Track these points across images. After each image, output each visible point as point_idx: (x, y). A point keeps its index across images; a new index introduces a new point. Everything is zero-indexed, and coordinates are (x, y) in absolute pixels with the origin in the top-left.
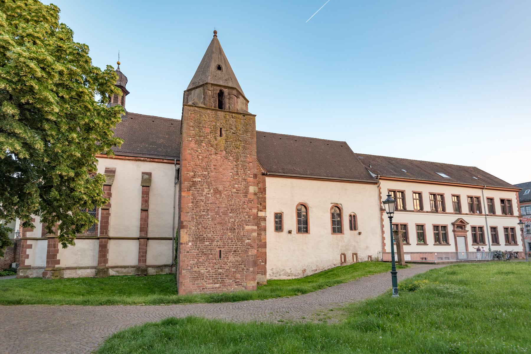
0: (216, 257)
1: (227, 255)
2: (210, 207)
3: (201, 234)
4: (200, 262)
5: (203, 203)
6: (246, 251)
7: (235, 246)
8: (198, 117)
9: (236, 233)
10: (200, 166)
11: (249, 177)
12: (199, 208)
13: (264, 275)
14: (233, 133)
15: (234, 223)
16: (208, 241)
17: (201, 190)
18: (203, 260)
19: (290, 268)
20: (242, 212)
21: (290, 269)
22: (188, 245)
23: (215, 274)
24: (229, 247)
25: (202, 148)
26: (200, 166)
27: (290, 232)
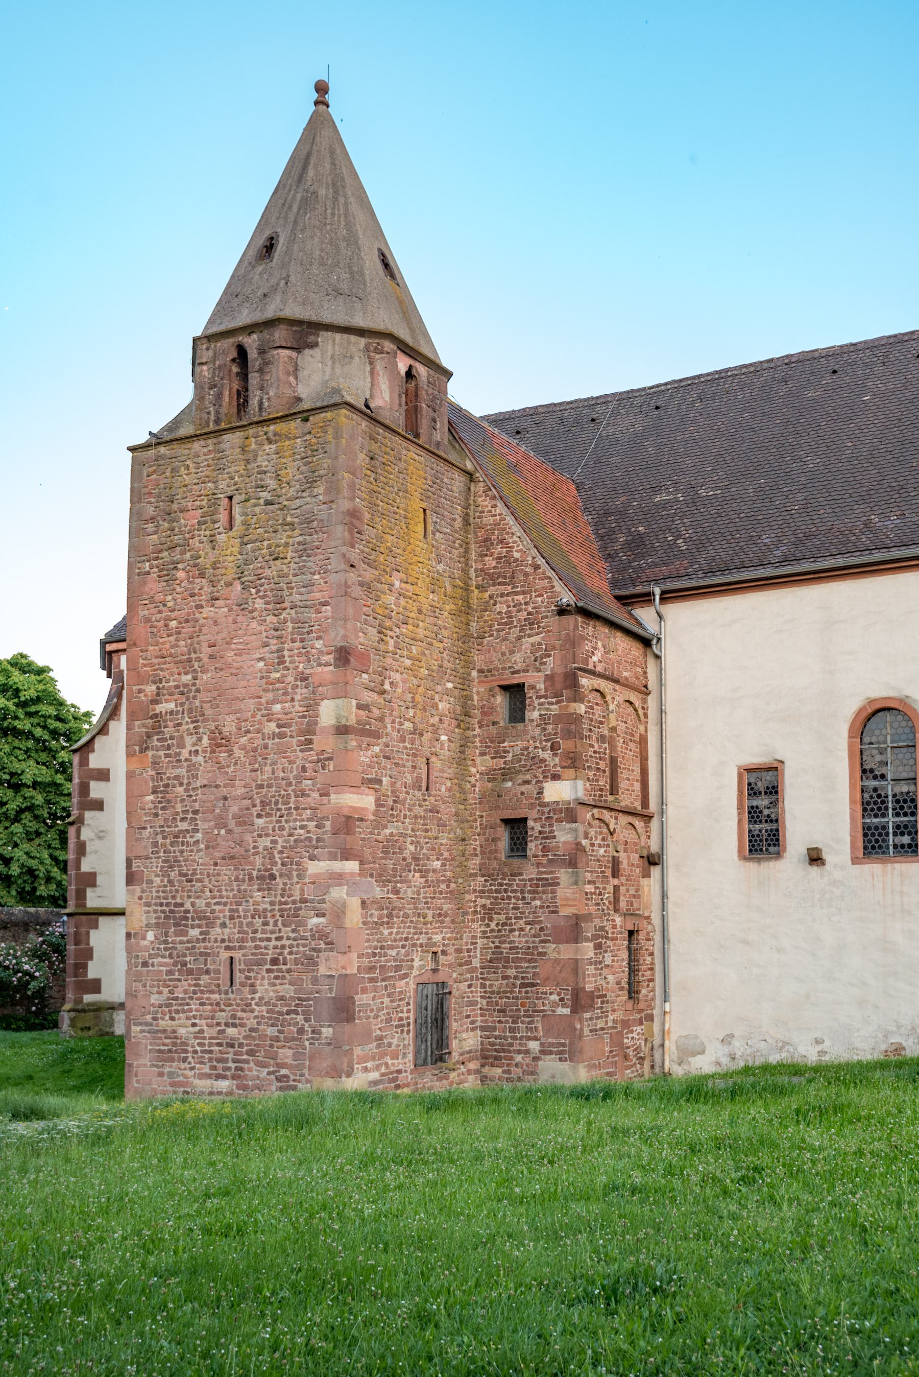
0: (220, 982)
1: (252, 974)
2: (200, 799)
3: (178, 900)
4: (176, 999)
5: (180, 790)
6: (312, 962)
7: (274, 943)
8: (166, 481)
9: (279, 892)
10: (171, 655)
11: (320, 665)
12: (172, 810)
13: (571, 1060)
14: (268, 503)
15: (269, 852)
16: (199, 926)
17: (174, 742)
18: (185, 992)
19: (818, 1035)
20: (297, 809)
21: (818, 1042)
22: (144, 938)
23: (219, 1044)
24: (256, 947)
25: (179, 589)
26: (171, 655)
27: (815, 858)
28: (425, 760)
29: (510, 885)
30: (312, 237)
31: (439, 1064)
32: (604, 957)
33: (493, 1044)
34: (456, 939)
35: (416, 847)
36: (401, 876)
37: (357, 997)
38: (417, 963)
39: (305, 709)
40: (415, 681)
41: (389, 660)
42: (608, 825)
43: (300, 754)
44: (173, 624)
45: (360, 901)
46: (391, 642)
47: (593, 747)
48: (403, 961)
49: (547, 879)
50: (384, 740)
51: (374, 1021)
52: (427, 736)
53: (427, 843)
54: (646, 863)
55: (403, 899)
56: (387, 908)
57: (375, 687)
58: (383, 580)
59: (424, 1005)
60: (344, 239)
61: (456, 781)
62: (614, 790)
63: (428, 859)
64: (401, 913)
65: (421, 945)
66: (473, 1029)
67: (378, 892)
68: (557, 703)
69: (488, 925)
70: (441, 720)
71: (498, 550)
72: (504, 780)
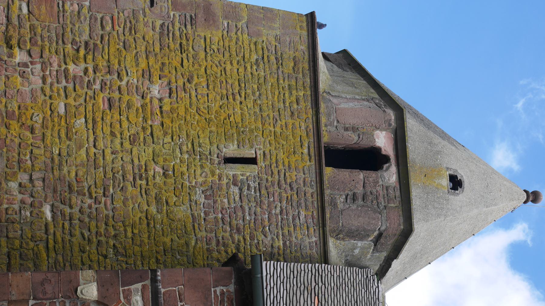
58: (152, 60)
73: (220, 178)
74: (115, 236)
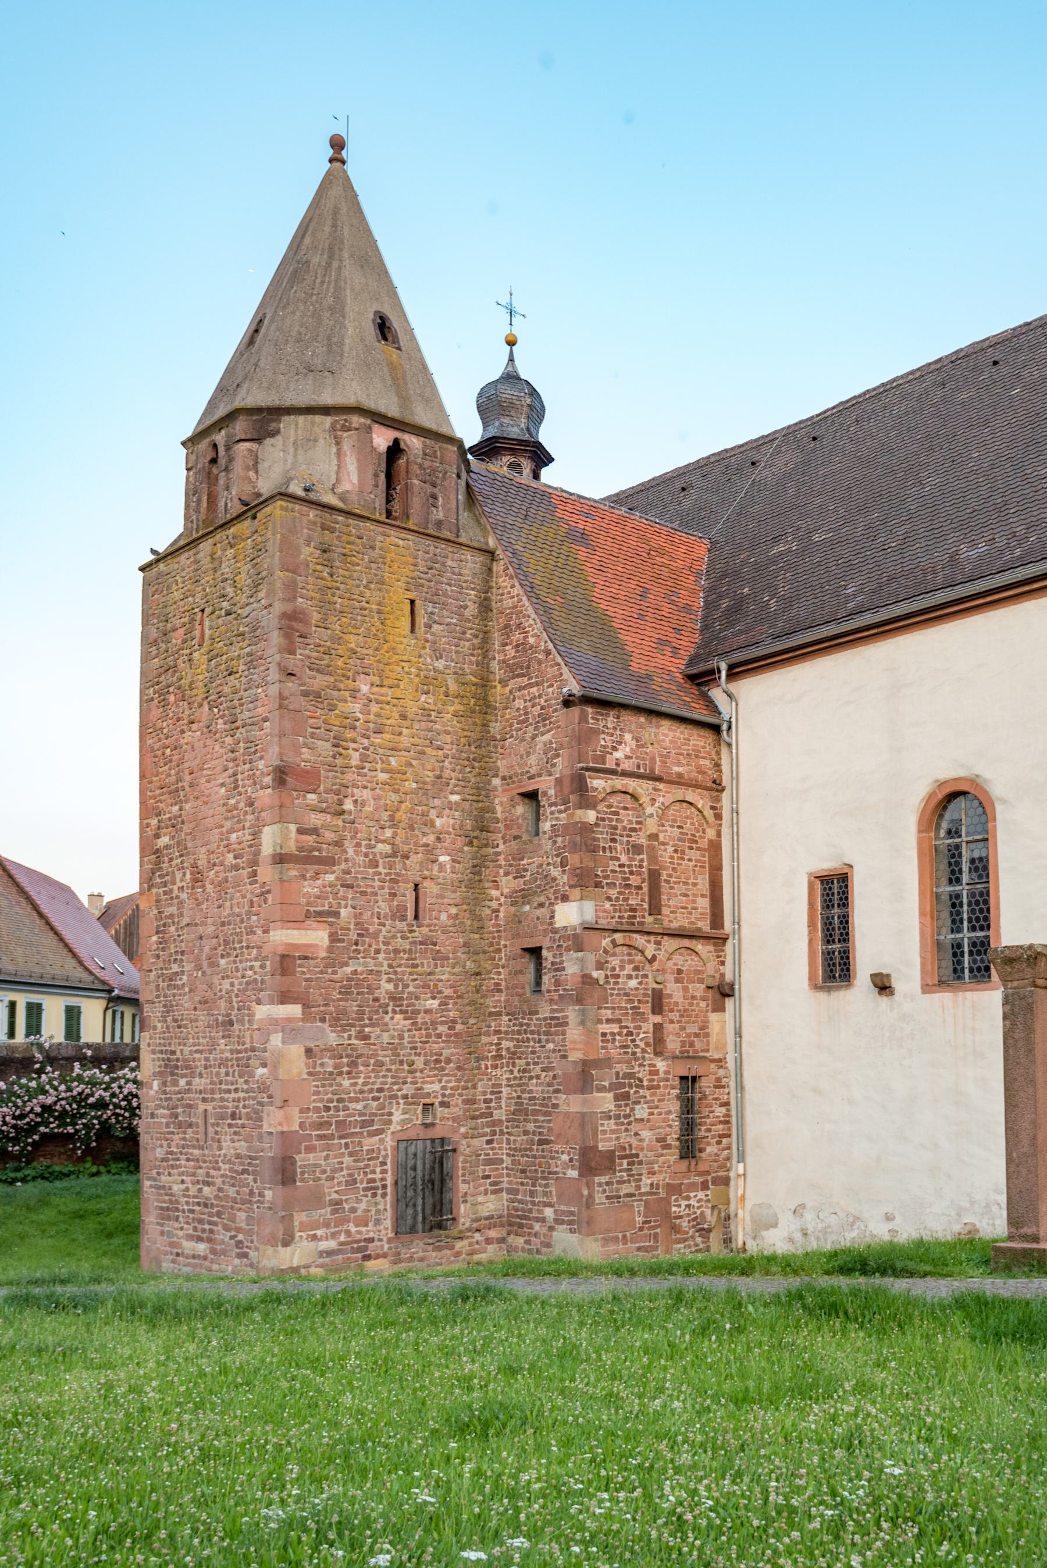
28: (411, 885)
29: (528, 1025)
30: (293, 313)
31: (436, 1232)
32: (632, 1110)
33: (516, 1210)
34: (466, 1088)
35: (396, 986)
36: (370, 1019)
37: (297, 1157)
38: (397, 1116)
39: (251, 837)
40: (394, 797)
41: (350, 776)
42: (642, 952)
43: (249, 887)
44: (168, 751)
45: (303, 1049)
46: (356, 756)
47: (618, 859)
48: (375, 1115)
49: (558, 1018)
50: (343, 866)
51: (327, 1184)
52: (415, 859)
53: (416, 980)
54: (718, 996)
55: (374, 1044)
56: (348, 1056)
57: (328, 807)
58: (342, 686)
59: (410, 1164)
60: (331, 309)
61: (465, 907)
62: (655, 909)
63: (417, 998)
64: (372, 1061)
65: (405, 1097)
66: (494, 1192)
67: (332, 1038)
68: (565, 811)
69: (512, 1072)
70: (438, 839)
71: (517, 637)
72: (523, 903)
73: (427, 641)
74: (470, 745)
